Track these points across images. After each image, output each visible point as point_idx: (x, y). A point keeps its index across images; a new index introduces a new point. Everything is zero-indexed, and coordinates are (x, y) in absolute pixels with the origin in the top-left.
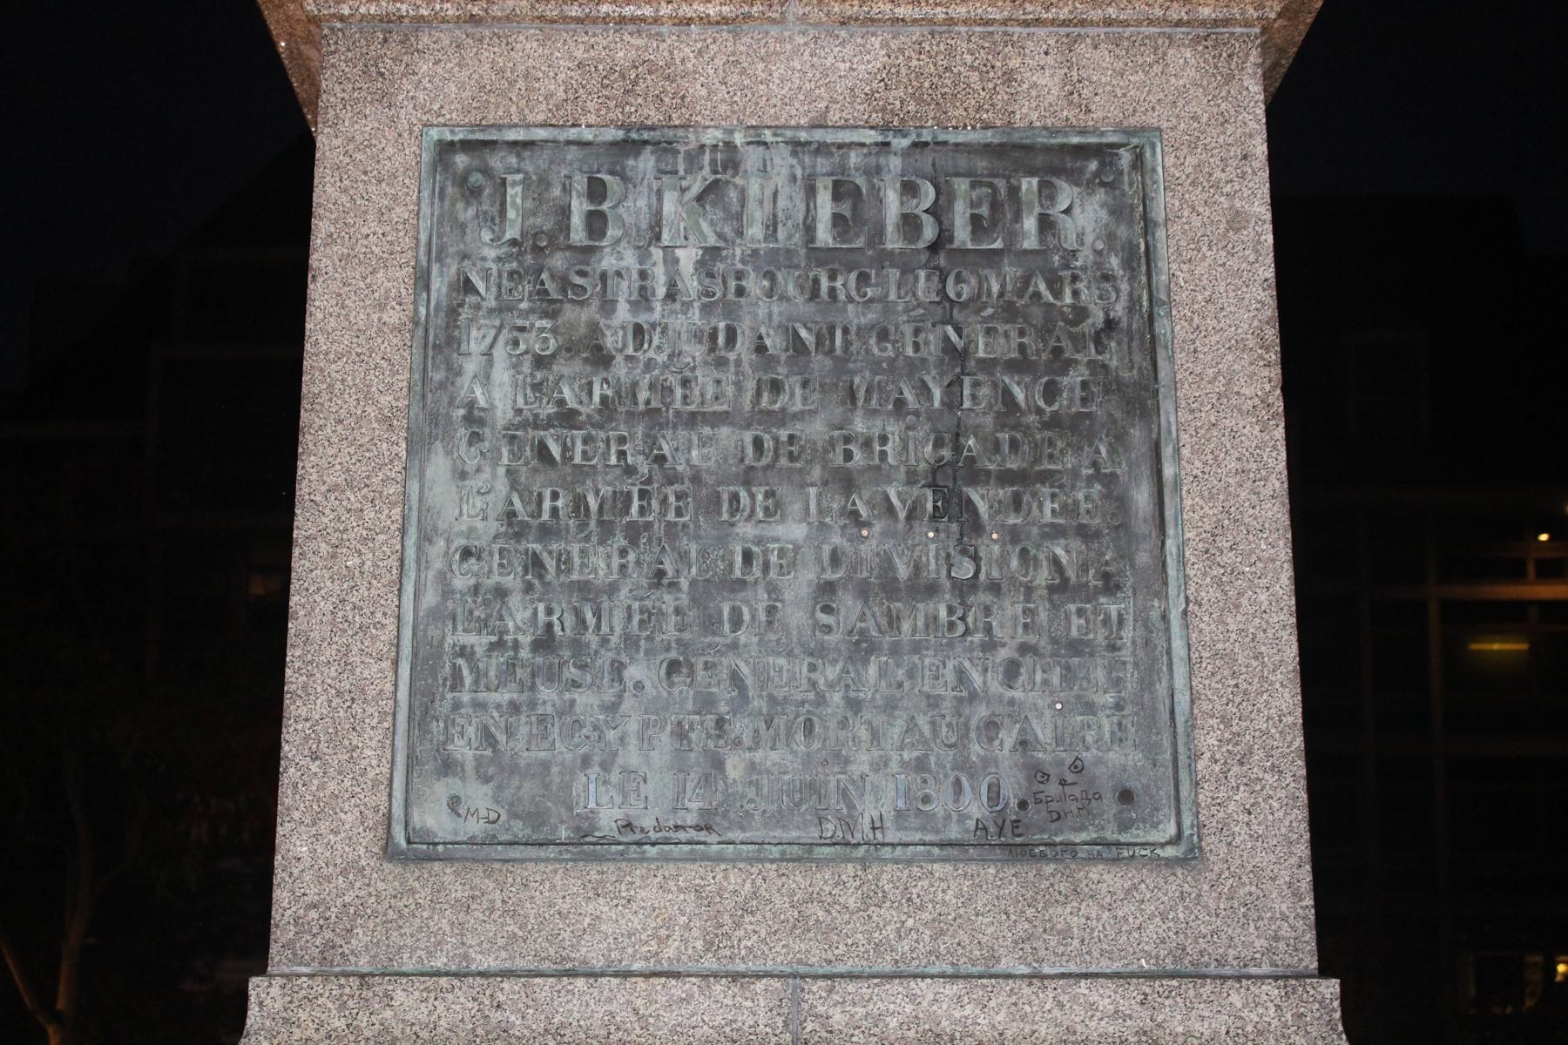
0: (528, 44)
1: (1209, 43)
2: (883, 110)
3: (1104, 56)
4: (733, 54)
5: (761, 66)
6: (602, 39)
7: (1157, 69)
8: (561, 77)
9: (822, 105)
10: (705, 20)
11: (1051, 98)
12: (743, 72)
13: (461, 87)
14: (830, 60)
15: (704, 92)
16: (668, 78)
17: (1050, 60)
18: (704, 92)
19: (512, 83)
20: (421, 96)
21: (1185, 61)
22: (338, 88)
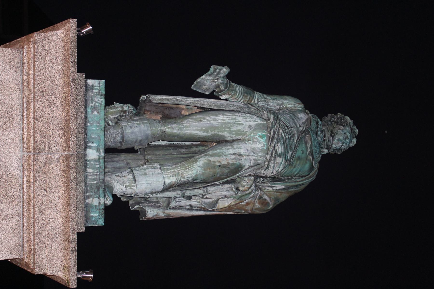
0: (17, 95)
1: (19, 247)
2: (3, 174)
3: (16, 223)
4: (16, 141)
5: (13, 147)
6: (19, 112)
7: (13, 235)
8: (10, 102)
9: (4, 160)
10: (23, 134)
11: (6, 212)
12: (11, 143)
13: (7, 80)
14: (14, 162)
15: (7, 134)
16: (10, 126)
17: (15, 211)
18: (7, 134)
19: (8, 91)
20: (5, 71)
21: (15, 241)
22: (7, 52)
